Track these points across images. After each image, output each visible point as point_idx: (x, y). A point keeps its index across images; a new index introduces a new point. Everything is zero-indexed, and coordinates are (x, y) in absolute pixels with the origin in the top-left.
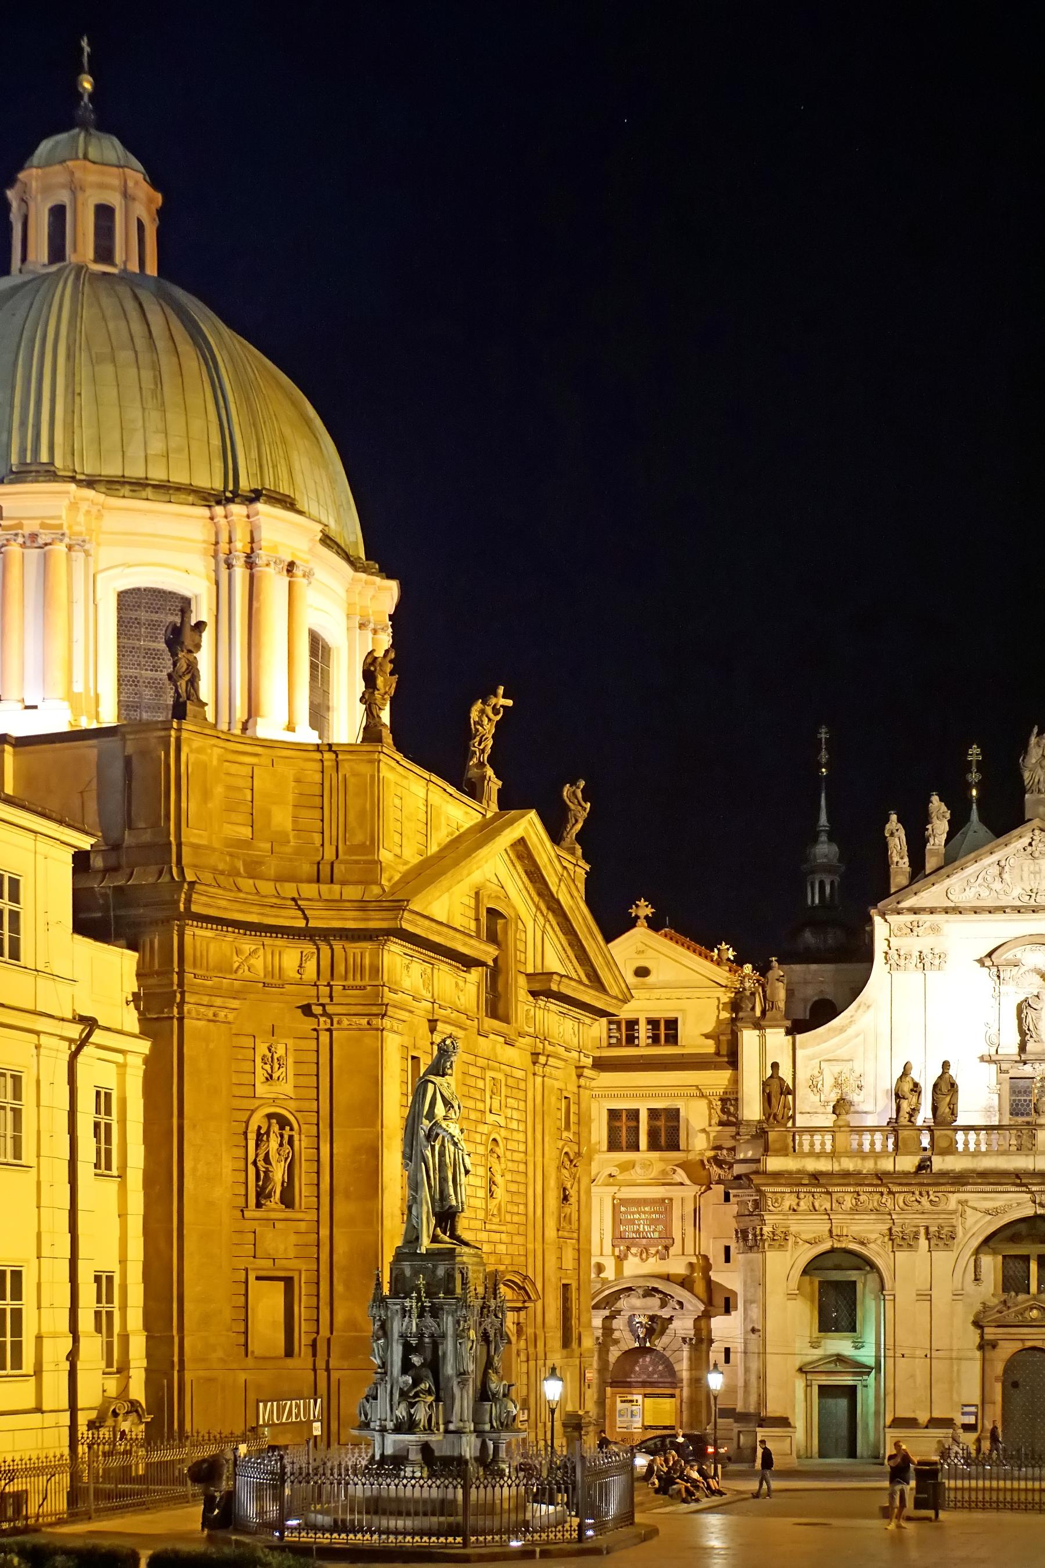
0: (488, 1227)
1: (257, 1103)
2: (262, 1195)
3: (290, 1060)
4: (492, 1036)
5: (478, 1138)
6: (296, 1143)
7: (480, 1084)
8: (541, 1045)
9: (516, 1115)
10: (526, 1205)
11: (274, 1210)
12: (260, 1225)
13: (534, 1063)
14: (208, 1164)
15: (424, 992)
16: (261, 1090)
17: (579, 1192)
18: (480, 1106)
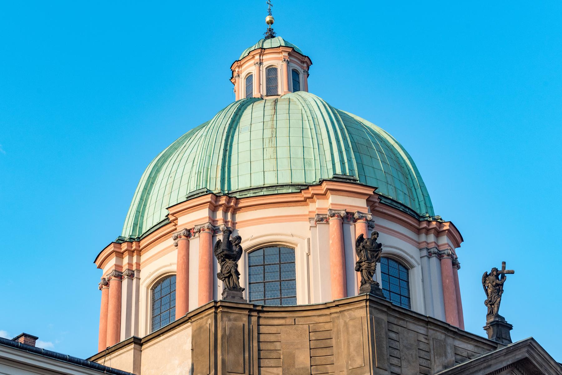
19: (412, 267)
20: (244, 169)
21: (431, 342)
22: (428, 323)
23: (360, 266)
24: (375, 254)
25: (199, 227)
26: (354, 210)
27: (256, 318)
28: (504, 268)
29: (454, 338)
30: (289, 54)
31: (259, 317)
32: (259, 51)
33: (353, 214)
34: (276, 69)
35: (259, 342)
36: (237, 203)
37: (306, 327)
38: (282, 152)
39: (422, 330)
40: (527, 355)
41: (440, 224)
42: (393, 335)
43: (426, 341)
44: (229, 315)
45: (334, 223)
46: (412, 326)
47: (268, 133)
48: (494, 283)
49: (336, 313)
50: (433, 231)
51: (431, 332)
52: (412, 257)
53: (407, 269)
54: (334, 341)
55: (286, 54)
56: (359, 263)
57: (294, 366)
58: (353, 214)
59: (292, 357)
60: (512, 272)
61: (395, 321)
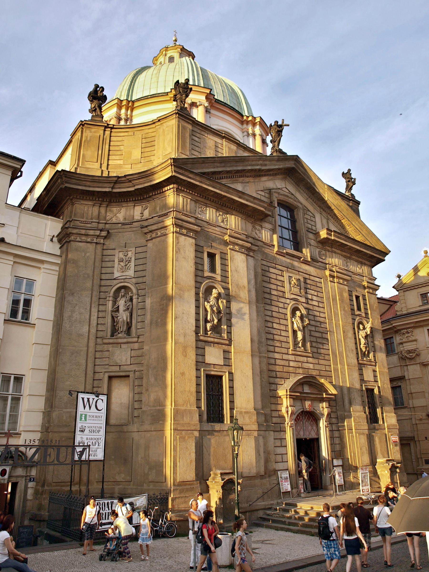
1: (115, 282)
3: (133, 259)
6: (135, 301)
9: (315, 298)
11: (120, 338)
12: (113, 347)
14: (81, 314)
16: (117, 274)
22: (224, 137)
23: (176, 98)
24: (186, 90)
25: (111, 118)
27: (109, 132)
28: (283, 122)
29: (243, 151)
30: (181, 50)
31: (111, 132)
32: (165, 49)
33: (196, 103)
34: (173, 58)
35: (110, 146)
36: (133, 105)
37: (140, 136)
40: (294, 166)
41: (255, 118)
42: (196, 139)
44: (91, 129)
48: (276, 130)
49: (159, 125)
50: (250, 122)
52: (237, 135)
54: (156, 142)
55: (180, 50)
56: (175, 96)
57: (131, 159)
58: (196, 103)
59: (130, 153)
60: (288, 125)
61: (199, 131)
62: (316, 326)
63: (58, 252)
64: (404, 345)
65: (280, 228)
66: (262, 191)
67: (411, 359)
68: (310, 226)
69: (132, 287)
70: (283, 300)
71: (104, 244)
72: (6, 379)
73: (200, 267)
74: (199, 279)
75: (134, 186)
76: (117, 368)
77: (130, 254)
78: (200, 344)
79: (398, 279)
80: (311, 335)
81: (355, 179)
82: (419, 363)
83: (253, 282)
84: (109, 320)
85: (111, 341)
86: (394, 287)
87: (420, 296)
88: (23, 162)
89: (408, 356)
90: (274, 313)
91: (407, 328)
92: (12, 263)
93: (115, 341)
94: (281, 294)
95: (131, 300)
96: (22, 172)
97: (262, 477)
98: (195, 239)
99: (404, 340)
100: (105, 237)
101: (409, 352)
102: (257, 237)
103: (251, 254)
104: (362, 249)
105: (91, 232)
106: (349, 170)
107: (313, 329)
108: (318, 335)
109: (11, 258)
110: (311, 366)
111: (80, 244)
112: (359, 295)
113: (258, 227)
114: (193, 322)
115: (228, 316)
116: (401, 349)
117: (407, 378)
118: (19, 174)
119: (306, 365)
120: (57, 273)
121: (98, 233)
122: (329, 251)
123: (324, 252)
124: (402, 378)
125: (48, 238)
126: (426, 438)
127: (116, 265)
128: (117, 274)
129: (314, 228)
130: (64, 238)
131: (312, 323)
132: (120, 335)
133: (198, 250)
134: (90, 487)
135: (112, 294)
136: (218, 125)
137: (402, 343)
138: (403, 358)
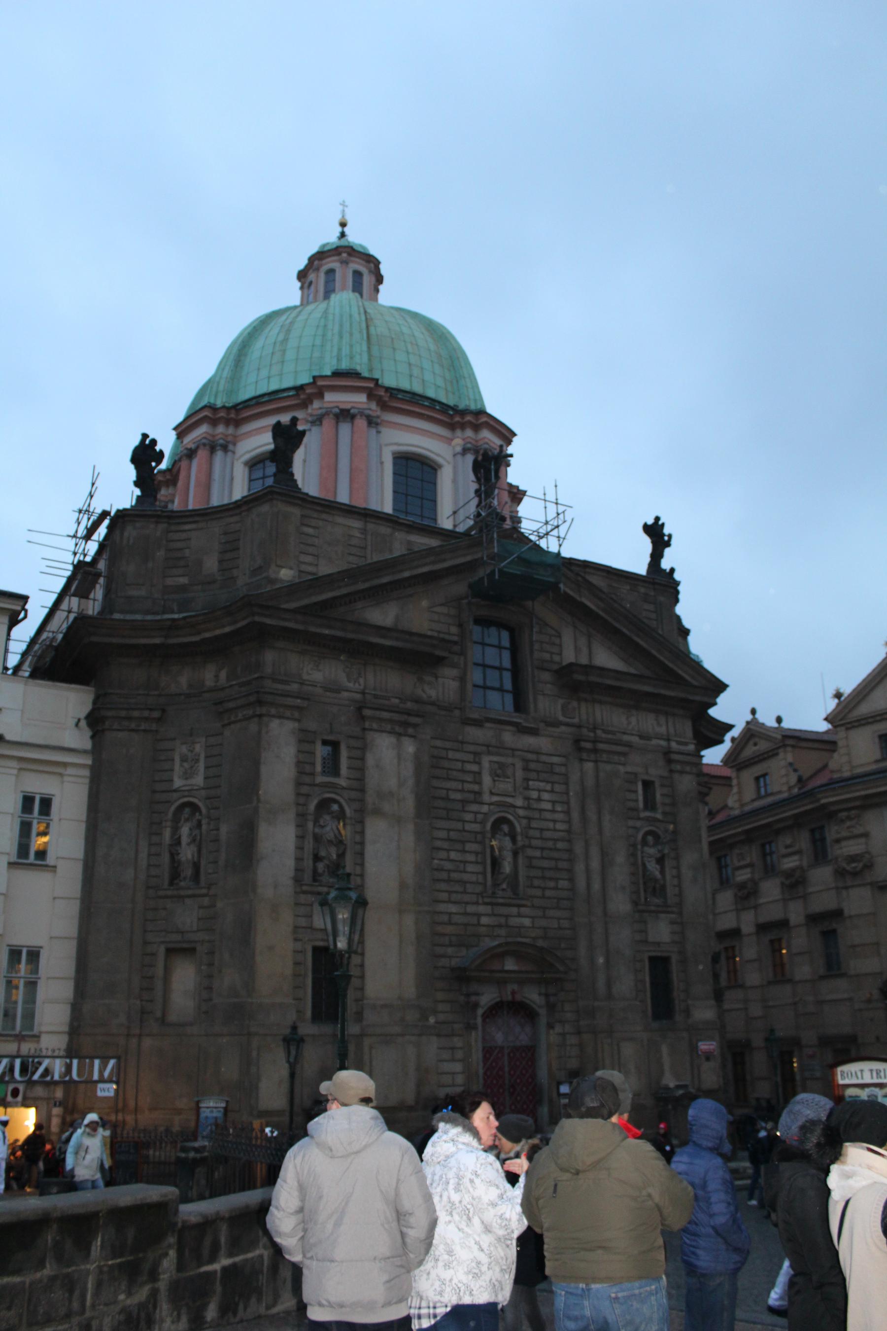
0: (487, 900)
1: (175, 795)
2: (175, 875)
4: (488, 725)
5: (469, 817)
6: (204, 827)
7: (475, 768)
8: (592, 734)
9: (546, 796)
10: (571, 880)
13: (580, 749)
15: (351, 685)
16: (178, 783)
17: (678, 868)
18: (476, 788)
19: (440, 466)
20: (252, 378)
21: (369, 537)
26: (348, 406)
29: (408, 532)
33: (348, 411)
38: (290, 355)
39: (356, 524)
42: (310, 531)
43: (363, 536)
45: (328, 423)
46: (340, 520)
47: (281, 337)
51: (370, 526)
53: (435, 470)
61: (315, 515)
62: (542, 849)
63: (88, 745)
64: (844, 843)
65: (480, 669)
66: (441, 605)
67: (855, 874)
68: (547, 656)
69: (200, 804)
70: (474, 807)
71: (157, 731)
72: (15, 954)
73: (308, 768)
74: (305, 790)
75: (199, 633)
76: (178, 937)
77: (198, 748)
78: (303, 898)
79: (836, 701)
80: (530, 866)
81: (670, 536)
82: (871, 884)
83: (411, 782)
84: (166, 858)
85: (169, 893)
86: (826, 719)
87: (877, 740)
88: (25, 599)
89: (848, 868)
90: (452, 833)
91: (849, 809)
92: (15, 772)
93: (175, 893)
94: (471, 797)
95: (199, 825)
96: (26, 611)
97: (411, 1109)
98: (299, 721)
99: (844, 834)
100: (159, 720)
101: (852, 859)
102: (424, 696)
103: (411, 731)
104: (656, 691)
105: (136, 714)
106: (657, 519)
107: (538, 853)
108: (545, 864)
109: (14, 764)
110: (527, 922)
111: (120, 735)
112: (652, 779)
113: (428, 678)
114: (291, 863)
115: (358, 847)
116: (839, 852)
117: (846, 912)
118: (22, 615)
119: (514, 921)
120: (87, 781)
121: (146, 713)
122: (586, 700)
123: (575, 704)
124: (837, 914)
125: (72, 722)
126: (878, 1038)
127: (177, 767)
128: (178, 783)
129: (556, 658)
130: (95, 721)
131: (535, 842)
132: (182, 884)
133: (305, 738)
134: (139, 1116)
135: (170, 815)
136: (396, 444)
137: (838, 841)
138: (840, 873)
